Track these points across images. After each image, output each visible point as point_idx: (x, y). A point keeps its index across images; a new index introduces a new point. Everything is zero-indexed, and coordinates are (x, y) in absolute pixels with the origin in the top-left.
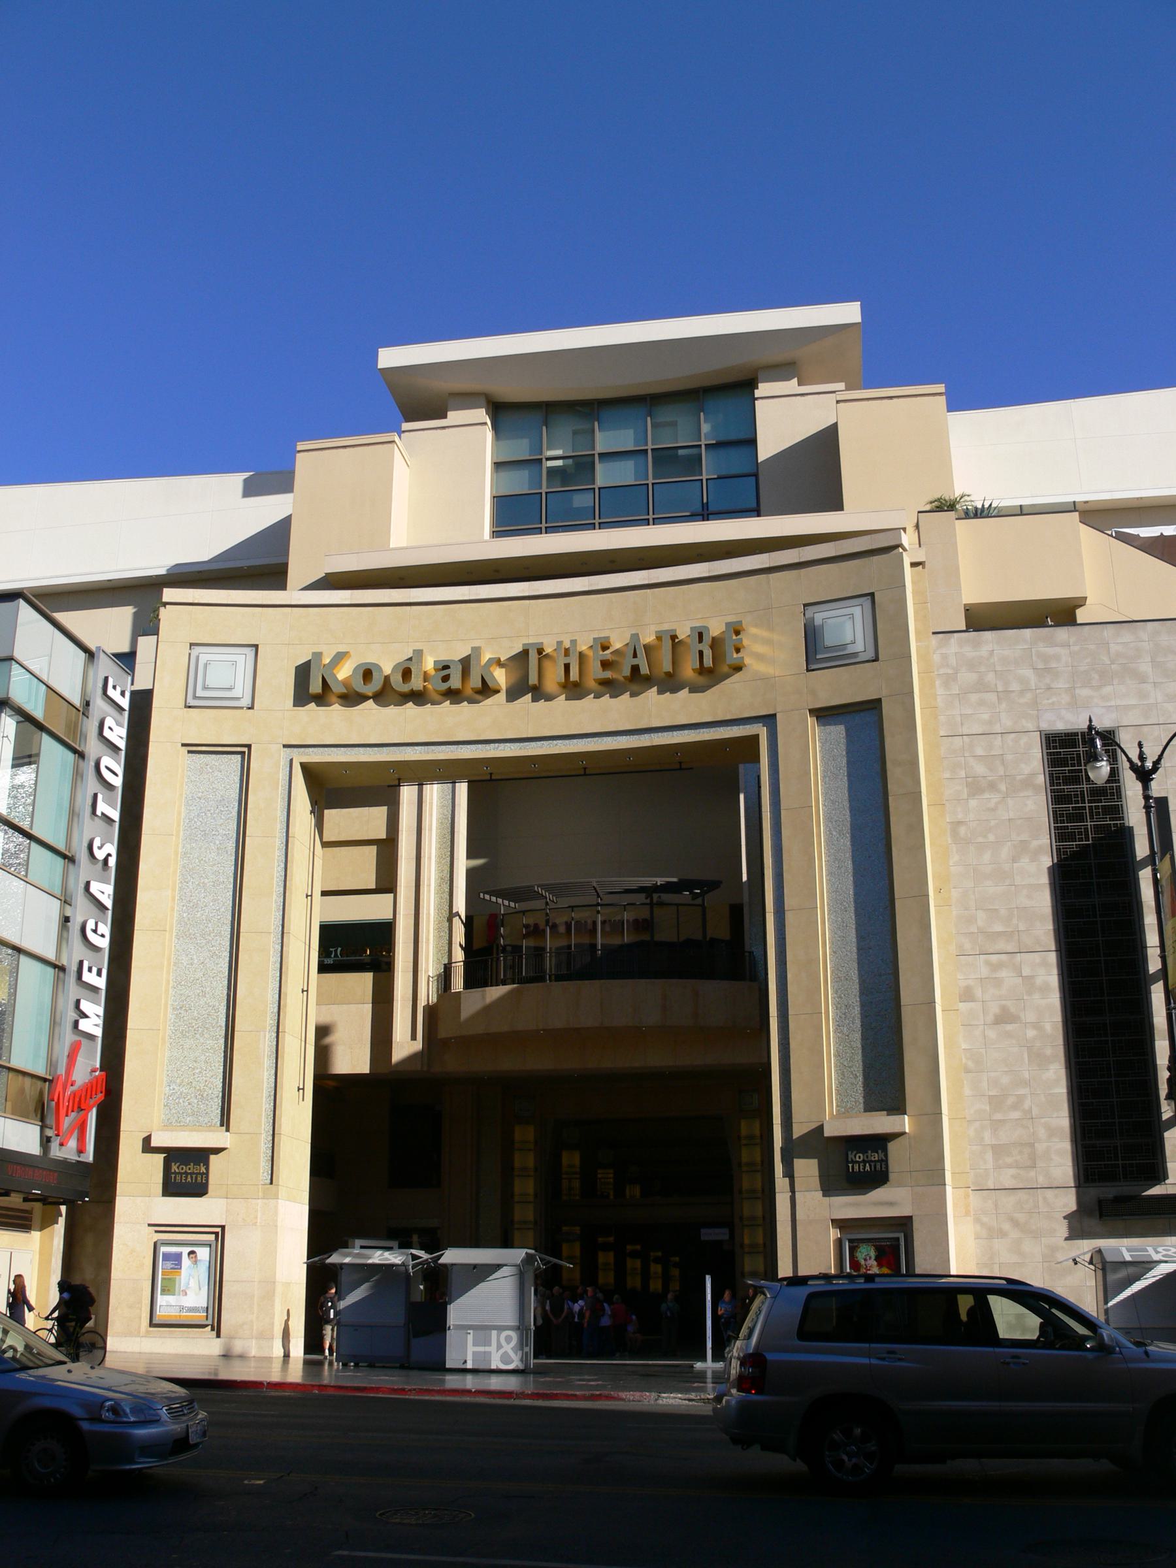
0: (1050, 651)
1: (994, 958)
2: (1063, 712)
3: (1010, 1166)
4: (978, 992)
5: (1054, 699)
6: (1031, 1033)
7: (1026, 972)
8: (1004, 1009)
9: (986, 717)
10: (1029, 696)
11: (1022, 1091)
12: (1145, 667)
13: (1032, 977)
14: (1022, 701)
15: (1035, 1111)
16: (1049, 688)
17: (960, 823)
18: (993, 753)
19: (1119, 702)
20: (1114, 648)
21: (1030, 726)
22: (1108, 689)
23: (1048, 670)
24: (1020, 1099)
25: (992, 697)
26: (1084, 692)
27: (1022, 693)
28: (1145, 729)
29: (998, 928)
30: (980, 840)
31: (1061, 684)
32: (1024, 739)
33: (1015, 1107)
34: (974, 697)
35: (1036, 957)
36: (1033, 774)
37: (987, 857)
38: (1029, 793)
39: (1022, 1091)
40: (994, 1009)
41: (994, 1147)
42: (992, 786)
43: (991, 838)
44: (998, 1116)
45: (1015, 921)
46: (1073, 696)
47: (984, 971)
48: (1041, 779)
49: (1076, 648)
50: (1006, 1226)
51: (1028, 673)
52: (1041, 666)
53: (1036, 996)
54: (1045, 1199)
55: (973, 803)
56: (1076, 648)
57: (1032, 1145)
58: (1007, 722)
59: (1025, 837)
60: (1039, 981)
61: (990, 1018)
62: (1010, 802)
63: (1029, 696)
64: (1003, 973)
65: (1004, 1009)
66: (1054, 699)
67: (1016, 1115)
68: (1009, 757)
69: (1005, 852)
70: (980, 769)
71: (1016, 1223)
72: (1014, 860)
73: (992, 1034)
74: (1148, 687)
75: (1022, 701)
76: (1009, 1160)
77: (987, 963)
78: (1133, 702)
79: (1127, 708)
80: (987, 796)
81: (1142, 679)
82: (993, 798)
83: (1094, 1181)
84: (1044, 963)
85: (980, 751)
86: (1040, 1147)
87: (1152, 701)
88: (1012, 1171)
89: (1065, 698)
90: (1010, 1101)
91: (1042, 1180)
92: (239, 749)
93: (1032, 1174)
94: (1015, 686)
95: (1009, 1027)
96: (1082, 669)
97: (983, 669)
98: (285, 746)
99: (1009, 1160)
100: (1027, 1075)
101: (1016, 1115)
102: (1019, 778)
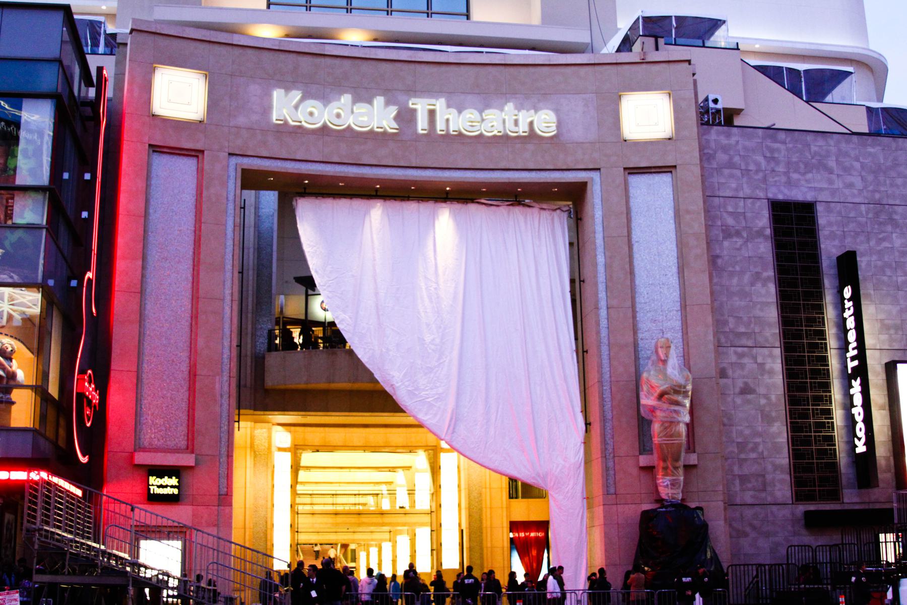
0: (776, 145)
1: (740, 350)
2: (782, 188)
3: (749, 490)
4: (730, 372)
5: (776, 179)
6: (763, 401)
7: (760, 360)
8: (746, 384)
9: (734, 185)
10: (761, 175)
11: (758, 440)
12: (832, 163)
13: (764, 364)
14: (756, 177)
15: (766, 453)
16: (773, 171)
17: (718, 257)
18: (739, 210)
19: (816, 185)
20: (814, 148)
21: (762, 195)
22: (809, 176)
23: (773, 158)
24: (756, 445)
25: (738, 173)
26: (795, 176)
27: (757, 171)
28: (833, 205)
29: (742, 329)
30: (730, 269)
31: (781, 169)
32: (758, 204)
33: (753, 450)
34: (726, 172)
35: (766, 351)
36: (764, 228)
37: (735, 281)
38: (761, 240)
39: (758, 440)
40: (740, 383)
41: (739, 476)
42: (738, 234)
43: (738, 268)
44: (743, 456)
45: (752, 326)
46: (789, 178)
47: (734, 359)
48: (768, 232)
49: (791, 146)
50: (748, 529)
51: (760, 159)
52: (768, 155)
53: (766, 377)
54: (772, 512)
55: (726, 244)
56: (791, 146)
57: (764, 476)
58: (747, 191)
59: (759, 269)
60: (767, 367)
61: (737, 390)
62: (750, 245)
63: (761, 175)
64: (746, 360)
65: (746, 384)
66: (776, 179)
67: (753, 455)
68: (749, 215)
69: (747, 278)
70: (730, 221)
71: (754, 528)
72: (752, 284)
73: (739, 401)
74: (834, 177)
75: (756, 177)
76: (750, 485)
77: (736, 353)
78: (826, 186)
79: (821, 189)
80: (735, 239)
81: (831, 172)
82: (740, 242)
83: (801, 500)
84: (771, 356)
85: (730, 209)
86: (769, 477)
87: (836, 186)
88: (751, 493)
89: (784, 179)
90: (750, 445)
91: (769, 499)
92: (193, 153)
93: (763, 495)
94: (752, 167)
95: (750, 397)
96: (794, 160)
97: (732, 153)
98: (230, 154)
99: (750, 485)
100: (760, 429)
101: (753, 455)
102: (755, 229)
